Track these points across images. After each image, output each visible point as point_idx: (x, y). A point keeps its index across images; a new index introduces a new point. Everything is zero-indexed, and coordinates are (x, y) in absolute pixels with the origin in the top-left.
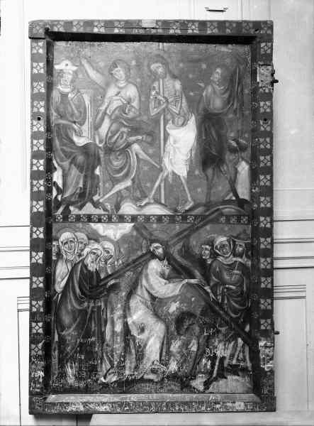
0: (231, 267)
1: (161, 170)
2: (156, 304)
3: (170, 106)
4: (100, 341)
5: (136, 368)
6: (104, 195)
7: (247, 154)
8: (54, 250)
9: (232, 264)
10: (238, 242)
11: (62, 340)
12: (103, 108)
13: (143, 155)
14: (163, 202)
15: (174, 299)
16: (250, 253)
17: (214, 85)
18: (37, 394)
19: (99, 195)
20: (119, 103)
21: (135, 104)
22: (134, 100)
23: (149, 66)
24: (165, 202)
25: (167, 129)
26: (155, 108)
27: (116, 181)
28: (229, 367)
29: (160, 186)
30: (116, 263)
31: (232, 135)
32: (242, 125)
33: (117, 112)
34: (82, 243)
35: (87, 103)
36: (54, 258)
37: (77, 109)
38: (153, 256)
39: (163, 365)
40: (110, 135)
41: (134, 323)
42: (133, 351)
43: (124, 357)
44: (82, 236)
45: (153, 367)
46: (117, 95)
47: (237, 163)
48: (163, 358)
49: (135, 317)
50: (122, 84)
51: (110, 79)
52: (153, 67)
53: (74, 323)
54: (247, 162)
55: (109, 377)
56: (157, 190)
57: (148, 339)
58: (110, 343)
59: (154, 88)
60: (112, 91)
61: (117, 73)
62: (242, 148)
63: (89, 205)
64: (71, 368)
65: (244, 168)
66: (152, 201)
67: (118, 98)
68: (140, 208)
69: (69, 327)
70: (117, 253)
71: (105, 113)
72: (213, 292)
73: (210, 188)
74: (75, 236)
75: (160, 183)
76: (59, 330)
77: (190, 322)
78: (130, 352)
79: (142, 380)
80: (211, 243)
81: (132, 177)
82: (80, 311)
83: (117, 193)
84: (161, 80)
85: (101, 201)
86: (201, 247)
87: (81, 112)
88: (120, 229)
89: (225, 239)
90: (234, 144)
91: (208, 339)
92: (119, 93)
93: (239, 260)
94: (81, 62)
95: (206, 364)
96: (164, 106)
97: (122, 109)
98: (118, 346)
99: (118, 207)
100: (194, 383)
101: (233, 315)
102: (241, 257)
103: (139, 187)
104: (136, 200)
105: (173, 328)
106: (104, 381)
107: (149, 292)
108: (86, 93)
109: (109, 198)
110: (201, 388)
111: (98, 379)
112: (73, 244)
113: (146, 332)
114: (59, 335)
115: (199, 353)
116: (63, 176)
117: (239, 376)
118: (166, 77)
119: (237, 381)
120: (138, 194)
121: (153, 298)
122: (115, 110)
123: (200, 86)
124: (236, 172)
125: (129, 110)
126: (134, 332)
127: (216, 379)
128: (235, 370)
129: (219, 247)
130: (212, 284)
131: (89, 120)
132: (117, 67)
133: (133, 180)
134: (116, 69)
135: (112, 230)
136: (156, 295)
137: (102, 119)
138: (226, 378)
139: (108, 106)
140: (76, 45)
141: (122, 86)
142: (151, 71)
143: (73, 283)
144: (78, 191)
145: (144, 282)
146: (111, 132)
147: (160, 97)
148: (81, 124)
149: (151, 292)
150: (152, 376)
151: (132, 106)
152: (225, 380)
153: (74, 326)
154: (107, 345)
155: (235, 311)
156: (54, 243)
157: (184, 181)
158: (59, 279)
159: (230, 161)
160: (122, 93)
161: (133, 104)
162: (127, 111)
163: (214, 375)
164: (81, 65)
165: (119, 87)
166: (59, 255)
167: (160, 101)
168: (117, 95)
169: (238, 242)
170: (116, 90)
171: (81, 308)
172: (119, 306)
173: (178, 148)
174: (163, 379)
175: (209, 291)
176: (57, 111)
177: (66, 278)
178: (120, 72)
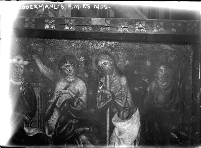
12: (53, 101)
22: (82, 94)
23: (97, 63)
25: (113, 122)
26: (102, 101)
31: (174, 128)
35: (38, 96)
40: (58, 126)
46: (66, 89)
59: (101, 84)
60: (61, 86)
67: (67, 91)
71: (54, 106)
84: (108, 77)
94: (32, 58)
97: (70, 101)
132: (66, 63)
134: (66, 65)
137: (52, 112)
142: (98, 67)
146: (60, 124)
160: (71, 88)
161: (81, 98)
165: (68, 81)
167: (106, 95)
170: (65, 84)
173: (122, 139)
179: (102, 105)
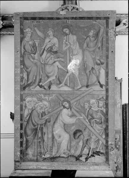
0: (97, 112)
1: (67, 72)
2: (66, 127)
3: (71, 46)
4: (43, 141)
5: (57, 152)
6: (44, 83)
7: (105, 65)
8: (24, 104)
9: (97, 111)
10: (100, 102)
11: (27, 141)
12: (43, 47)
13: (60, 66)
14: (68, 85)
15: (73, 124)
16: (105, 106)
17: (90, 37)
18: (18, 161)
19: (42, 82)
20: (50, 45)
21: (57, 45)
24: (69, 85)
27: (48, 77)
28: (96, 152)
29: (67, 79)
30: (49, 110)
31: (98, 58)
32: (102, 53)
33: (49, 49)
34: (35, 102)
35: (37, 45)
36: (24, 108)
37: (33, 48)
38: (64, 107)
39: (68, 151)
40: (46, 58)
41: (56, 134)
42: (56, 145)
43: (52, 147)
44: (35, 99)
45: (64, 152)
47: (100, 69)
48: (68, 148)
49: (57, 132)
50: (51, 37)
51: (46, 36)
52: (65, 30)
53: (32, 133)
54: (104, 69)
55: (46, 156)
56: (66, 81)
57: (62, 140)
58: (46, 142)
59: (65, 39)
60: (47, 40)
61: (49, 33)
62: (102, 64)
63: (38, 87)
64: (31, 151)
65: (103, 72)
66: (64, 85)
67: (50, 43)
68: (58, 88)
69: (30, 136)
70: (49, 106)
72: (89, 122)
73: (88, 79)
74: (32, 99)
75: (68, 77)
76: (26, 136)
77: (80, 134)
78: (55, 146)
79: (59, 157)
80: (89, 102)
81: (56, 75)
82: (34, 129)
83: (49, 82)
85: (43, 85)
86: (84, 104)
87: (34, 49)
88: (51, 96)
89: (95, 100)
90: (99, 62)
91: (87, 141)
92: (50, 41)
93: (100, 109)
94: (34, 29)
95: (86, 151)
96: (69, 46)
97: (51, 48)
98: (50, 144)
99: (49, 87)
100: (81, 159)
101: (98, 132)
102: (101, 108)
103: (58, 79)
104: (58, 84)
105: (72, 136)
106: (44, 157)
107: (62, 122)
108: (37, 41)
109: (46, 84)
110: (84, 160)
111: (42, 156)
112: (31, 102)
113: (62, 138)
114: (26, 139)
115: (83, 146)
116: (27, 75)
117: (100, 156)
118: (69, 34)
119: (99, 158)
120: (58, 82)
121: (65, 124)
122: (49, 48)
123: (85, 38)
124: (99, 73)
125: (54, 48)
126: (56, 137)
127: (90, 157)
128: (98, 153)
129: (92, 104)
130: (89, 119)
131: (38, 52)
133: (56, 76)
134: (49, 31)
135: (47, 97)
136: (65, 123)
137: (43, 52)
138: (95, 157)
139: (46, 46)
140: (33, 22)
141: (51, 38)
142: (63, 32)
143: (31, 118)
144: (33, 81)
145: (61, 118)
146: (47, 57)
147: (67, 43)
148: (35, 54)
149: (64, 122)
150: (63, 155)
151: (56, 47)
152: (94, 157)
153: (32, 135)
154: (45, 143)
155: (99, 130)
156: (24, 102)
157: (77, 77)
158: (25, 116)
159: (97, 68)
162: (53, 49)
163: (90, 155)
164: (35, 30)
166: (26, 107)
167: (67, 44)
168: (49, 42)
169: (100, 102)
170: (49, 40)
171: (34, 128)
172: (50, 127)
174: (68, 157)
175: (88, 121)
176: (24, 48)
177: (29, 116)
178: (50, 33)
179: (66, 48)
